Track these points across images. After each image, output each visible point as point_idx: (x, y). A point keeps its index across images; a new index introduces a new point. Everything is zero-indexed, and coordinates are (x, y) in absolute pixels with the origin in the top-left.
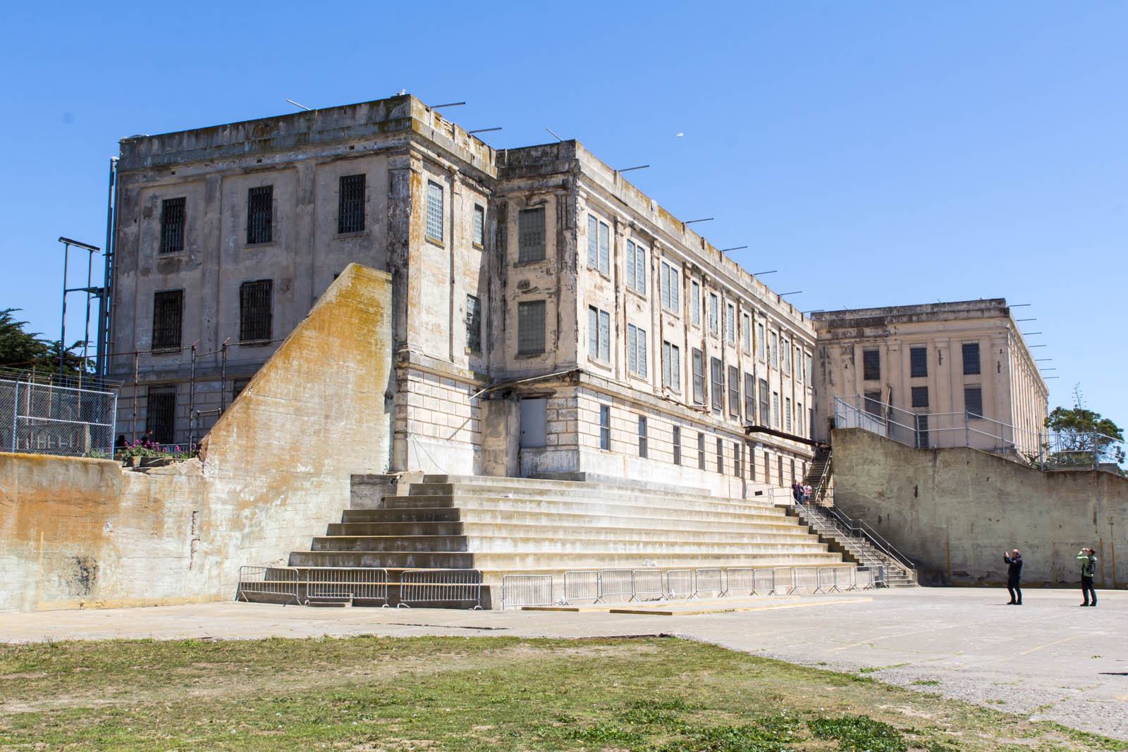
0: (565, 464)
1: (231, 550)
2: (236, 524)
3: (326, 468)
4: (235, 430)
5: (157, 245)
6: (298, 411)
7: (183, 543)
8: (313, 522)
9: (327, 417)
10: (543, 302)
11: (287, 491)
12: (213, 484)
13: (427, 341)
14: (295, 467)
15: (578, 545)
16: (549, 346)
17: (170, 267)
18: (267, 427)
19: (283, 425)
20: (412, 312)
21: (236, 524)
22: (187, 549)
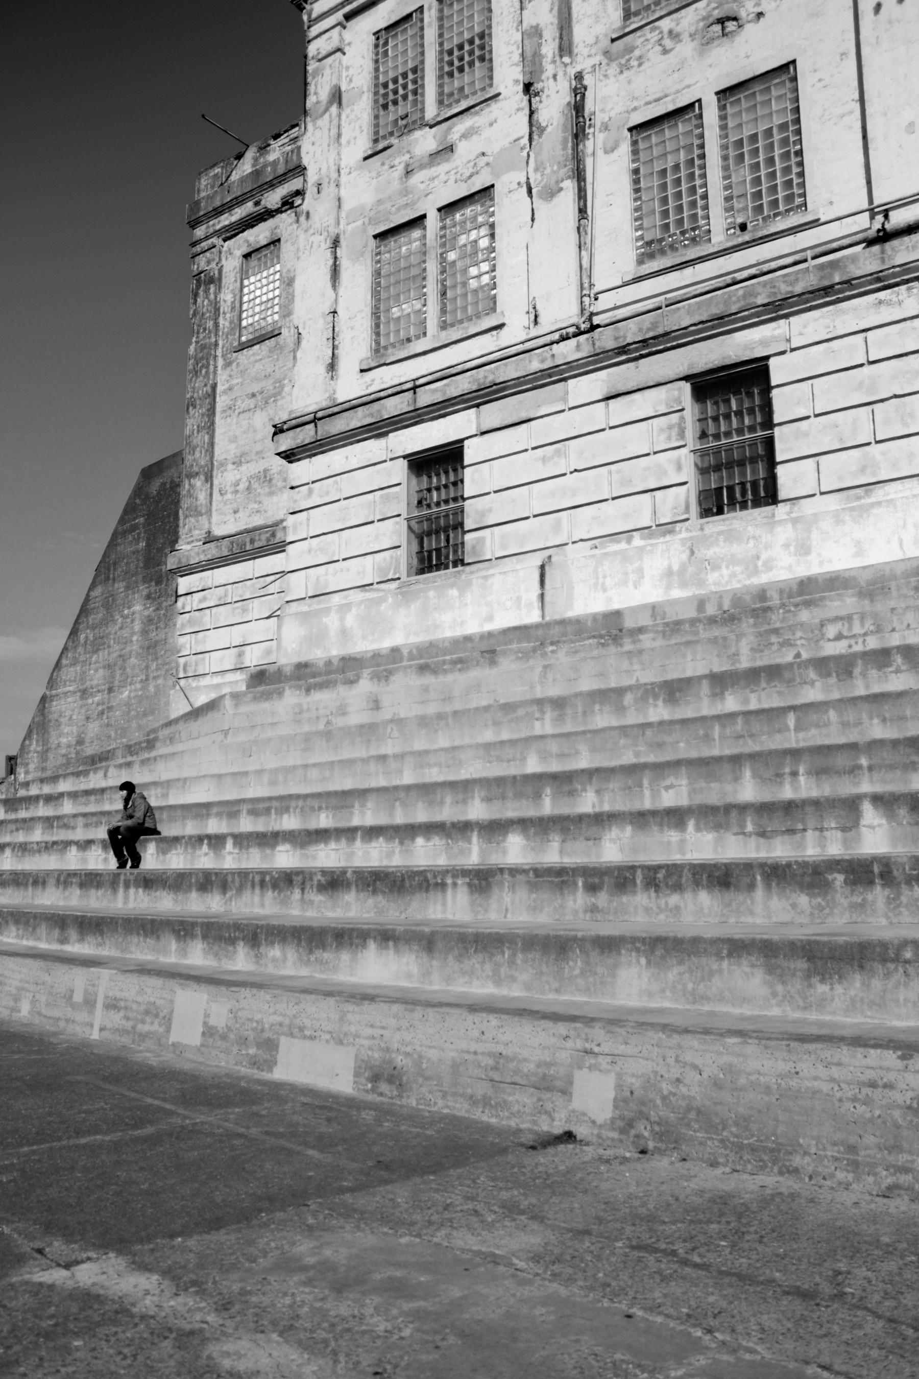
13: (235, 512)
18: (58, 723)
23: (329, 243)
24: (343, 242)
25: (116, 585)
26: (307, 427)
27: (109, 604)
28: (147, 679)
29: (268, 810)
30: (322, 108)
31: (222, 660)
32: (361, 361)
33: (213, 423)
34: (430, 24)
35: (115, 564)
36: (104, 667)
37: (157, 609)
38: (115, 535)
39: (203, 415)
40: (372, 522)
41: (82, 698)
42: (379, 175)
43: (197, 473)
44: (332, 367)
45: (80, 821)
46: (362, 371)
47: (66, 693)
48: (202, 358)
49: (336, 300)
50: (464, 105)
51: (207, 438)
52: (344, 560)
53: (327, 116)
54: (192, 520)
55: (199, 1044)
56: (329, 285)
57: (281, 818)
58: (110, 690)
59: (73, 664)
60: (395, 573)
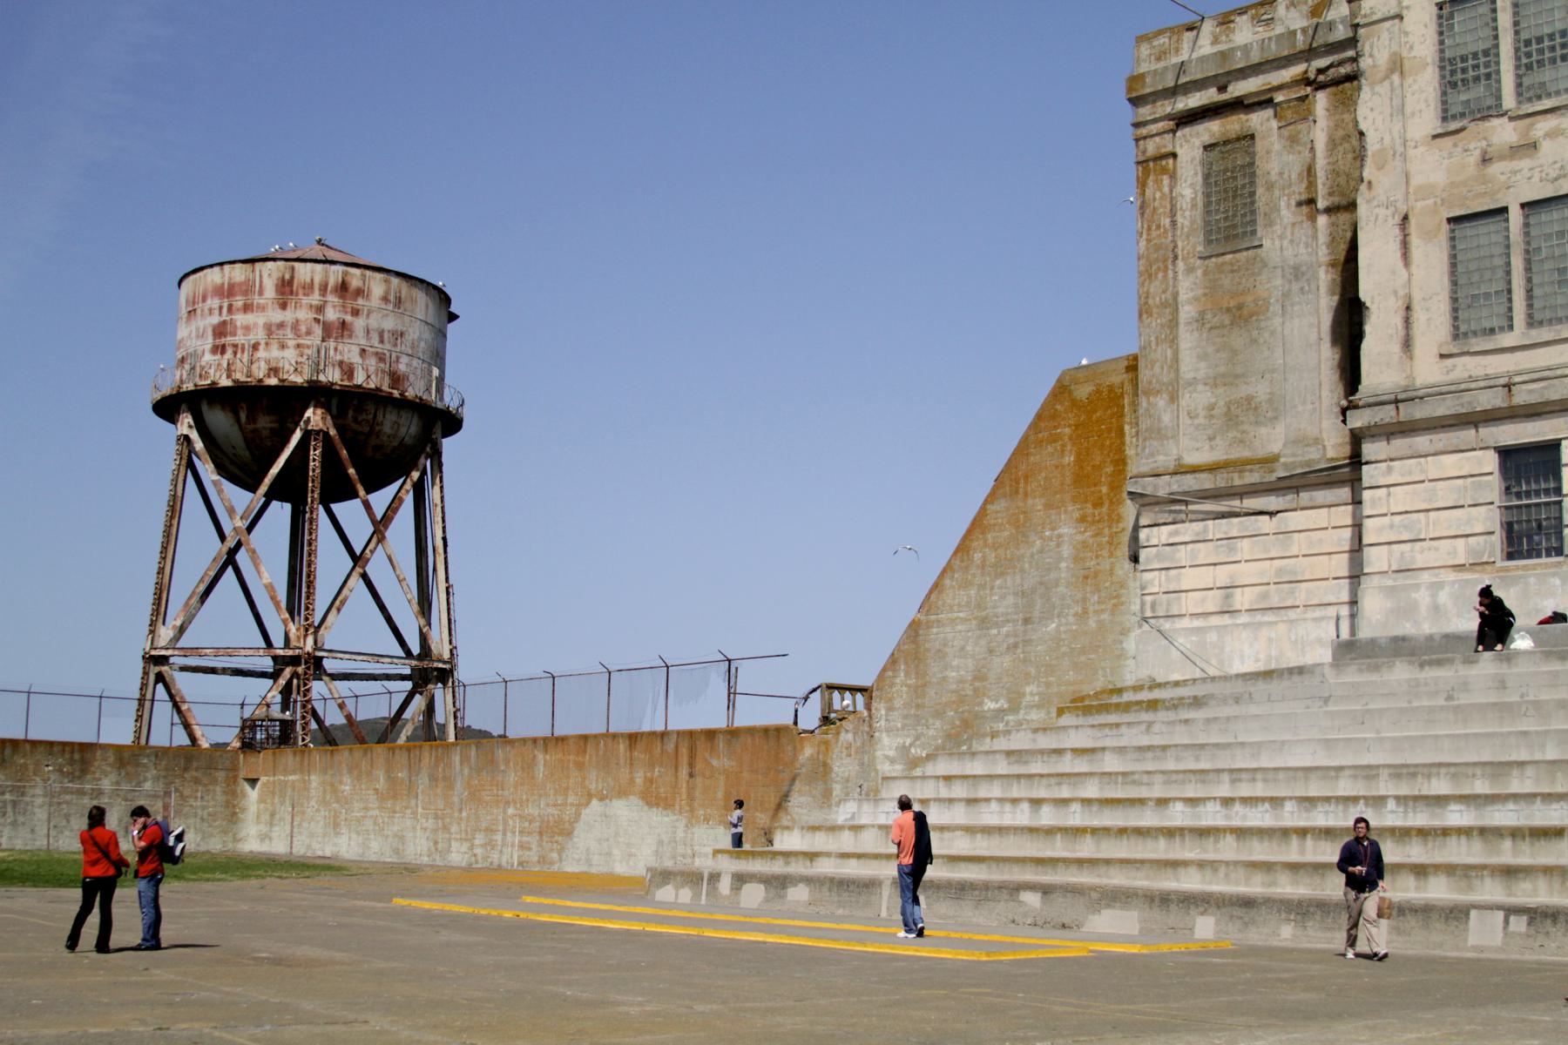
3: (1028, 698)
4: (902, 667)
11: (970, 739)
14: (981, 704)
15: (1076, 807)
18: (941, 654)
19: (963, 648)
23: (1398, 219)
24: (1413, 220)
25: (1030, 502)
26: (1387, 407)
27: (1022, 526)
28: (1085, 611)
29: (1414, 775)
30: (1380, 75)
31: (1203, 600)
32: (1440, 346)
33: (1176, 337)
34: (1504, 9)
35: (1026, 477)
36: (1015, 594)
37: (1097, 535)
38: (1025, 440)
39: (1162, 326)
40: (1463, 506)
41: (980, 627)
42: (1450, 156)
43: (1158, 392)
44: (1407, 344)
45: (1158, 778)
46: (1442, 356)
47: (952, 621)
48: (1157, 260)
49: (1409, 280)
50: (1547, 103)
51: (1169, 353)
52: (1431, 539)
53: (1387, 83)
54: (1155, 443)
55: (1500, 944)
56: (1400, 263)
57: (1429, 782)
58: (1027, 621)
59: (966, 585)
60: (1489, 557)
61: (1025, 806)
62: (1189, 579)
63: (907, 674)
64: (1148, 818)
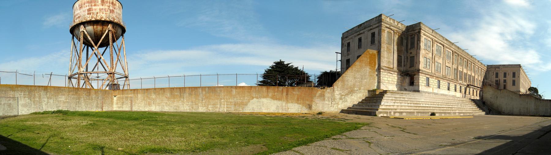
0: (417, 89)
1: (340, 103)
2: (341, 99)
5: (346, 51)
6: (355, 78)
7: (329, 102)
8: (359, 99)
9: (362, 79)
10: (414, 56)
11: (353, 93)
12: (336, 92)
15: (412, 104)
16: (415, 65)
17: (348, 55)
18: (347, 81)
19: (351, 81)
20: (382, 58)
21: (341, 99)
22: (330, 103)
25: (363, 64)
35: (362, 61)
61: (407, 104)
62: (386, 79)
63: (341, 83)
64: (419, 105)
